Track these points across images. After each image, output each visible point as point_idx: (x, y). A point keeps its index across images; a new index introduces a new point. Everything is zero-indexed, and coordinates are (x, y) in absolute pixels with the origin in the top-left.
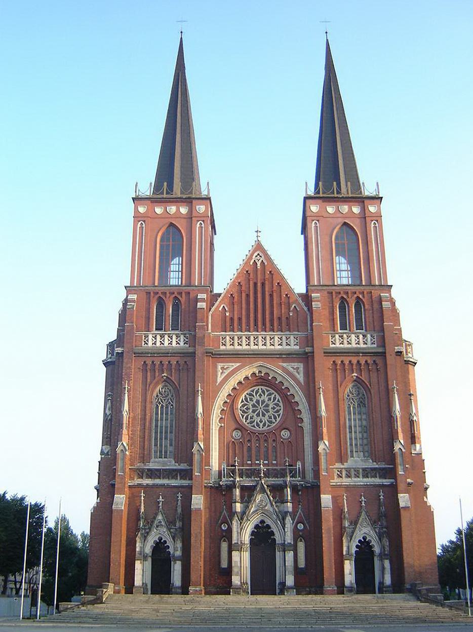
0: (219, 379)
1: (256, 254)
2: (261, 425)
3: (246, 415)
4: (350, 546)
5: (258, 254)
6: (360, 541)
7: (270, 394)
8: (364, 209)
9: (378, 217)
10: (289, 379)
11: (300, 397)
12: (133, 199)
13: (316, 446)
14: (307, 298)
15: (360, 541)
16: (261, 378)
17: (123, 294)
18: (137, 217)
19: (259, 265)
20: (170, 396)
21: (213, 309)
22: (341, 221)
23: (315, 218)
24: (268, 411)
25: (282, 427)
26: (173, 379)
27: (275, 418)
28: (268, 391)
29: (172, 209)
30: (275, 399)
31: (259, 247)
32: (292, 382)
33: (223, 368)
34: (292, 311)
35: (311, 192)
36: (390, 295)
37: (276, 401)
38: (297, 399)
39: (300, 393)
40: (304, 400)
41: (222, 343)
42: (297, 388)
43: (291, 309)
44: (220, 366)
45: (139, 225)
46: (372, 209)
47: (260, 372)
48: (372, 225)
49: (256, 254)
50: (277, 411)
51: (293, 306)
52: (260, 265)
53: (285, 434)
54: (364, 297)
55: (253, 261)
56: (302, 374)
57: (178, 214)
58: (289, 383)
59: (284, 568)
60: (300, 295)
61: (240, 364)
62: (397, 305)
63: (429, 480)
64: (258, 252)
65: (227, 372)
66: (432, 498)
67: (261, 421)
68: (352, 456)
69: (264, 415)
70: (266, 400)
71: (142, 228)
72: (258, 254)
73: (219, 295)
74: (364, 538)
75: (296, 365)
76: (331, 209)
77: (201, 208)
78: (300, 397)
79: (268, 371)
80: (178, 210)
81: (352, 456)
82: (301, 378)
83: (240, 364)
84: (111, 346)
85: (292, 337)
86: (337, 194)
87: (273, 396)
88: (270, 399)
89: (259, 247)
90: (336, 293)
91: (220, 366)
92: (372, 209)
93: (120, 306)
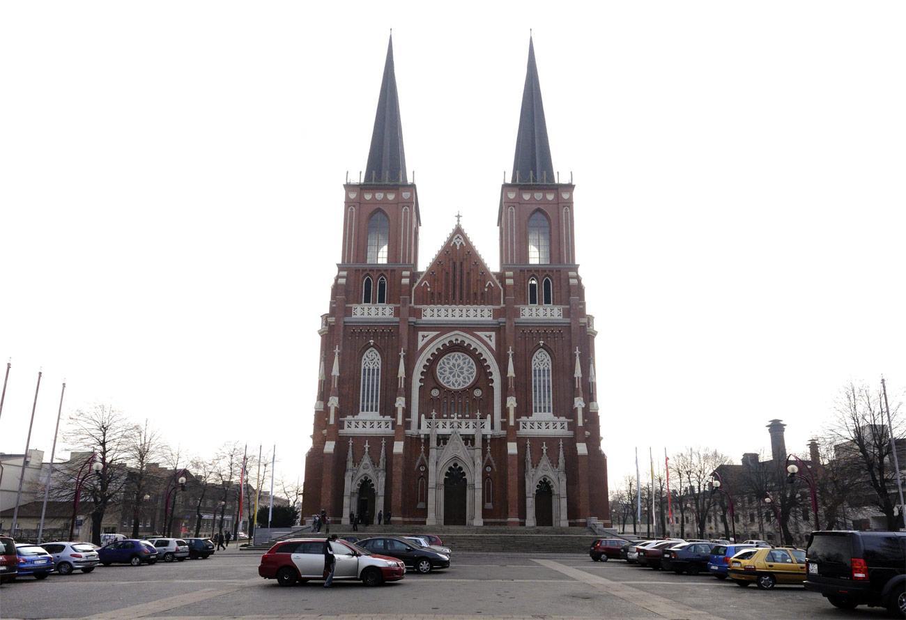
1: (456, 237)
2: (456, 384)
3: (443, 376)
4: (531, 487)
5: (458, 237)
6: (540, 482)
7: (465, 359)
8: (558, 197)
9: (569, 204)
10: (483, 346)
11: (491, 362)
12: (344, 185)
13: (504, 402)
14: (501, 277)
15: (540, 482)
16: (458, 345)
17: (335, 271)
18: (348, 203)
19: (458, 245)
20: (376, 359)
21: (416, 285)
22: (535, 207)
23: (511, 204)
24: (462, 373)
25: (474, 386)
26: (378, 344)
27: (469, 379)
28: (463, 356)
29: (379, 196)
30: (469, 362)
31: (458, 231)
32: (485, 348)
33: (424, 337)
34: (488, 287)
35: (509, 181)
36: (577, 273)
37: (470, 365)
38: (488, 363)
39: (492, 358)
40: (495, 364)
42: (489, 353)
43: (487, 286)
44: (420, 334)
45: (349, 210)
46: (565, 196)
47: (457, 340)
48: (564, 210)
49: (456, 237)
50: (471, 373)
52: (460, 246)
53: (478, 393)
54: (553, 275)
55: (453, 243)
57: (385, 200)
58: (482, 349)
60: (495, 274)
61: (438, 333)
62: (583, 282)
63: (602, 433)
64: (458, 235)
65: (426, 340)
66: (604, 447)
67: (456, 382)
68: (536, 411)
69: (459, 376)
70: (461, 364)
71: (352, 212)
72: (458, 237)
73: (422, 273)
74: (545, 479)
75: (488, 333)
76: (526, 197)
77: (406, 195)
78: (491, 362)
79: (464, 339)
80: (385, 196)
81: (536, 411)
82: (493, 344)
83: (438, 333)
84: (325, 317)
85: (486, 310)
86: (533, 182)
87: (467, 360)
88: (465, 363)
89: (458, 231)
90: (528, 271)
91: (420, 334)
92: (565, 196)
93: (333, 282)
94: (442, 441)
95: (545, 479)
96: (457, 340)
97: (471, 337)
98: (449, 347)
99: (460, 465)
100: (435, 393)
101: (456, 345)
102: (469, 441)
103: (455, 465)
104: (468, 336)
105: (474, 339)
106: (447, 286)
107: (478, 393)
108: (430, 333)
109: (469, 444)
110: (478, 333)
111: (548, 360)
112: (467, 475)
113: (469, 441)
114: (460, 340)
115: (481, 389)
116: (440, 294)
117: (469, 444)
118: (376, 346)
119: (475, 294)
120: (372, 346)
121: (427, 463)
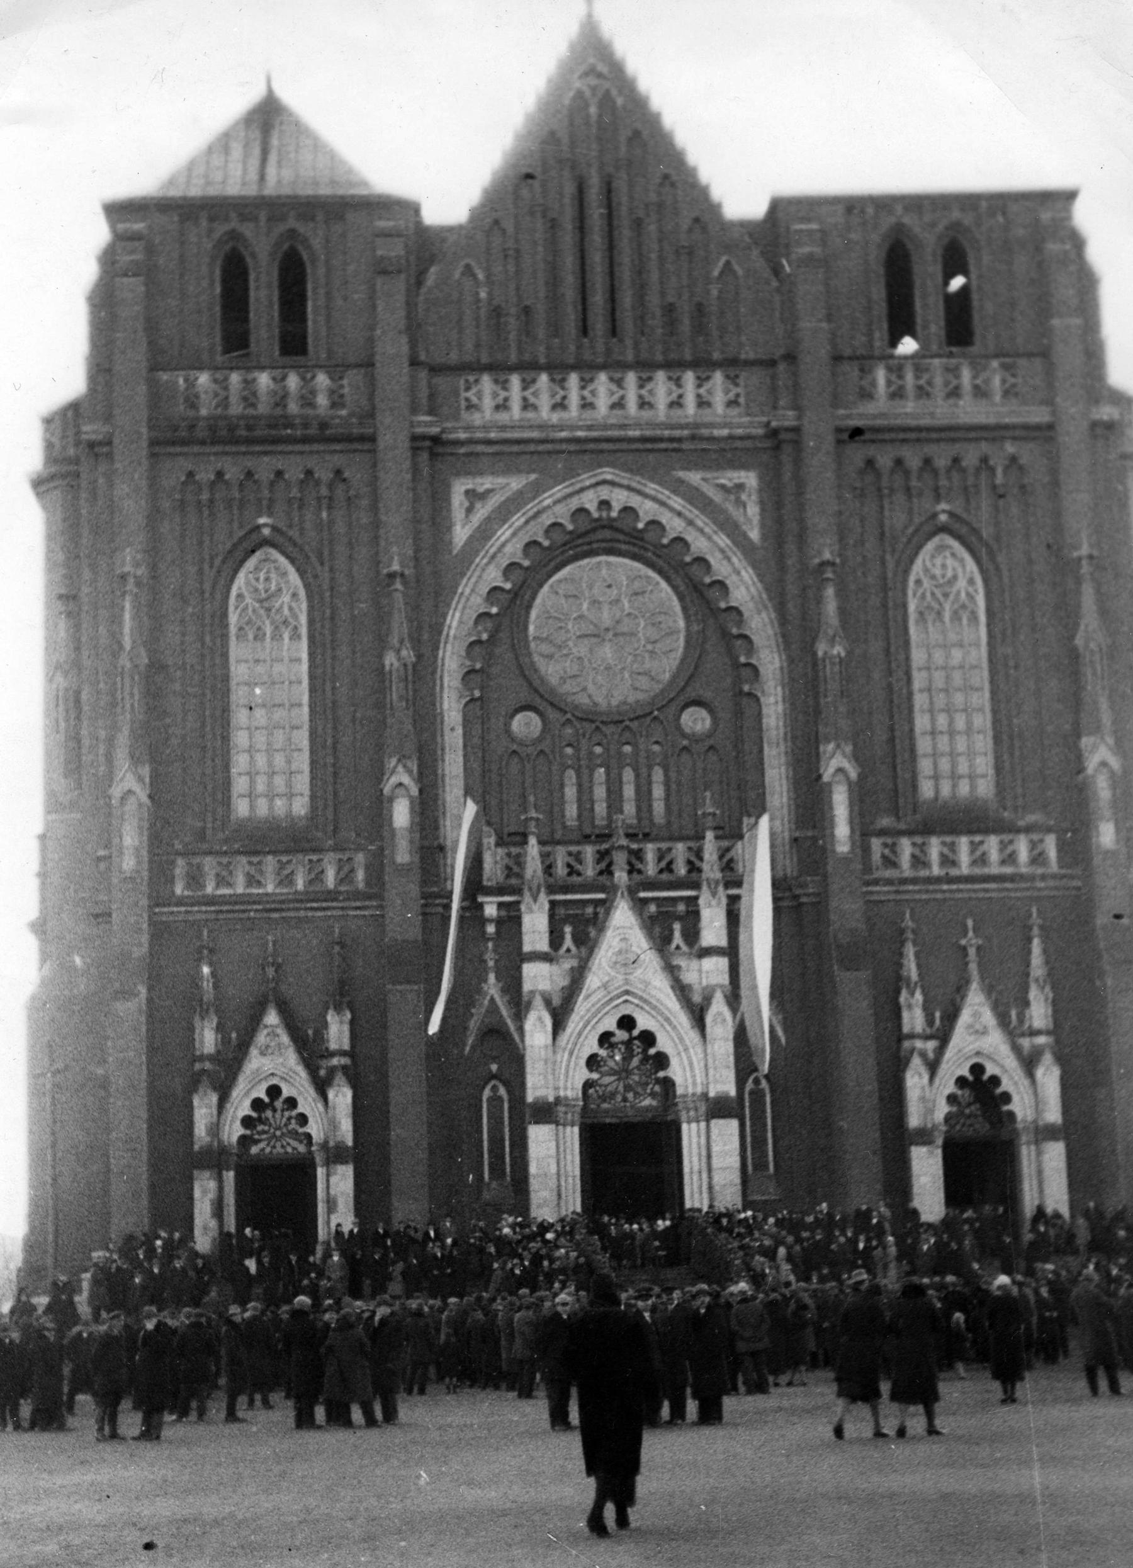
0: (461, 534)
39: (748, 575)
41: (467, 400)
47: (605, 504)
51: (721, 263)
53: (696, 721)
56: (753, 510)
59: (705, 1176)
74: (977, 1069)
94: (568, 929)
95: (977, 1069)
96: (605, 504)
97: (664, 494)
98: (575, 535)
99: (643, 1022)
100: (526, 725)
101: (600, 525)
102: (677, 927)
103: (627, 1022)
104: (652, 488)
105: (677, 502)
106: (554, 282)
107: (696, 721)
108: (501, 480)
109: (677, 939)
110: (694, 477)
111: (971, 581)
112: (674, 1062)
113: (677, 927)
114: (616, 507)
115: (711, 711)
116: (527, 311)
117: (677, 939)
118: (280, 540)
119: (669, 310)
120: (266, 542)
121: (511, 1026)
